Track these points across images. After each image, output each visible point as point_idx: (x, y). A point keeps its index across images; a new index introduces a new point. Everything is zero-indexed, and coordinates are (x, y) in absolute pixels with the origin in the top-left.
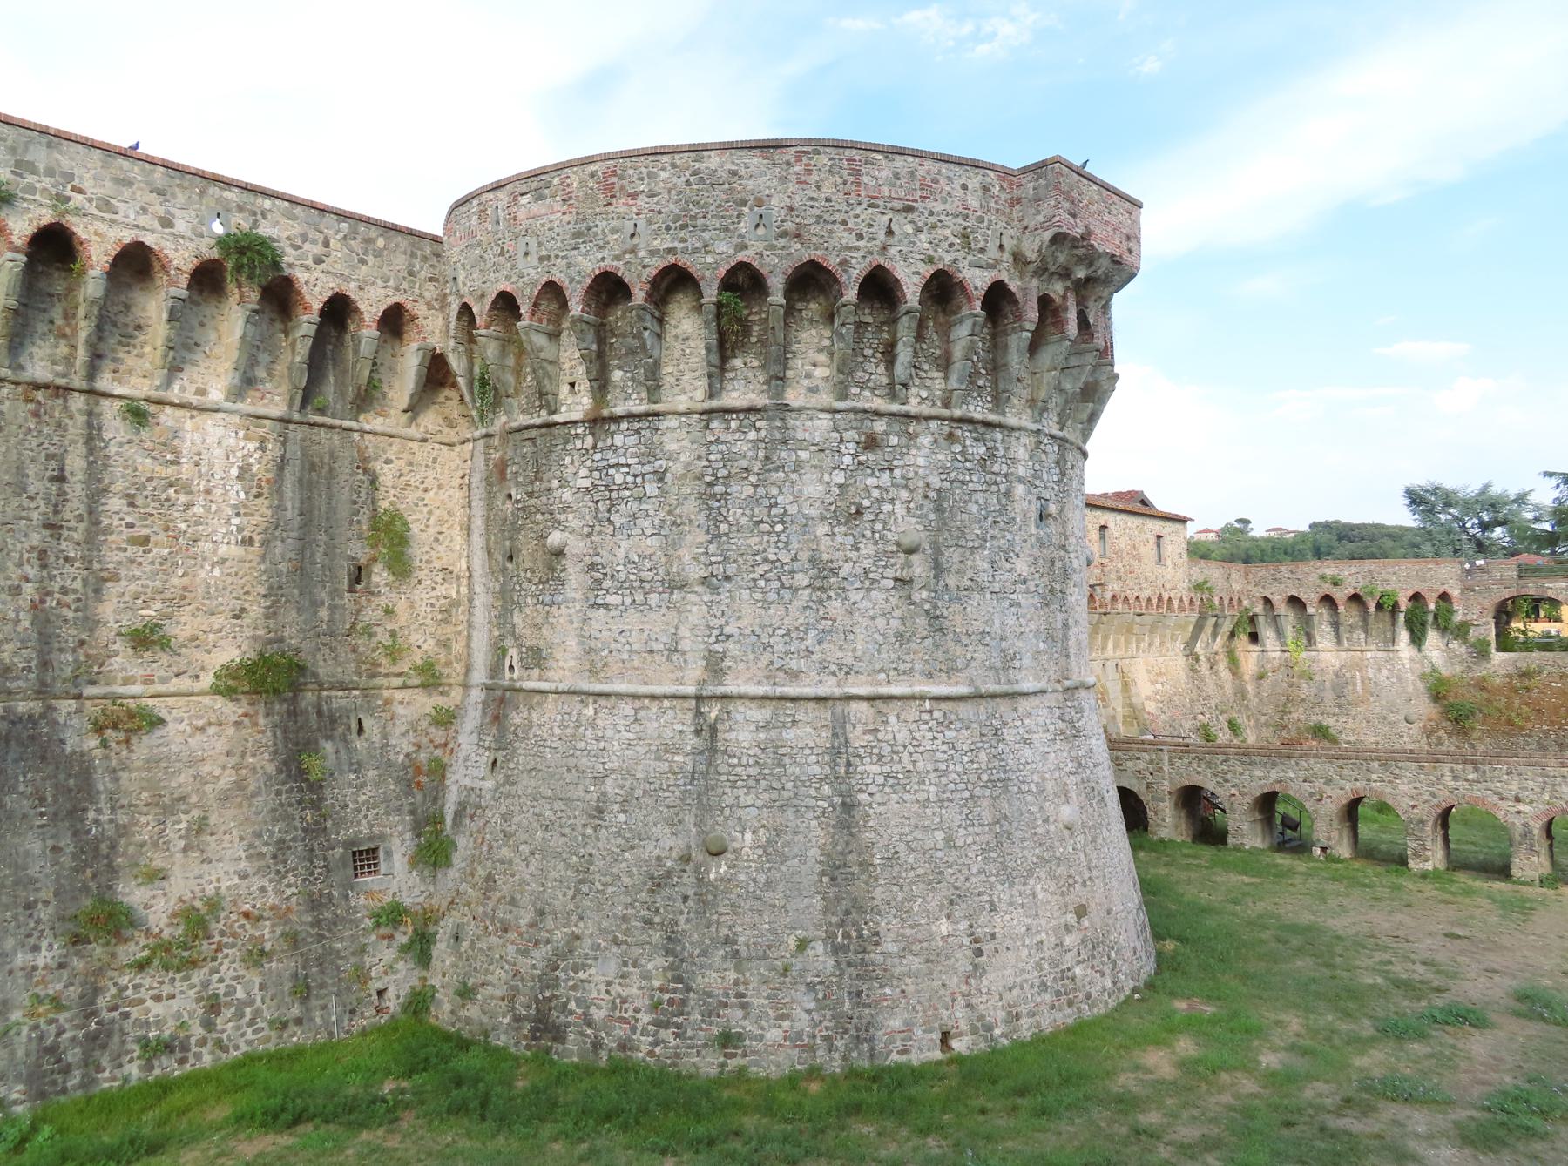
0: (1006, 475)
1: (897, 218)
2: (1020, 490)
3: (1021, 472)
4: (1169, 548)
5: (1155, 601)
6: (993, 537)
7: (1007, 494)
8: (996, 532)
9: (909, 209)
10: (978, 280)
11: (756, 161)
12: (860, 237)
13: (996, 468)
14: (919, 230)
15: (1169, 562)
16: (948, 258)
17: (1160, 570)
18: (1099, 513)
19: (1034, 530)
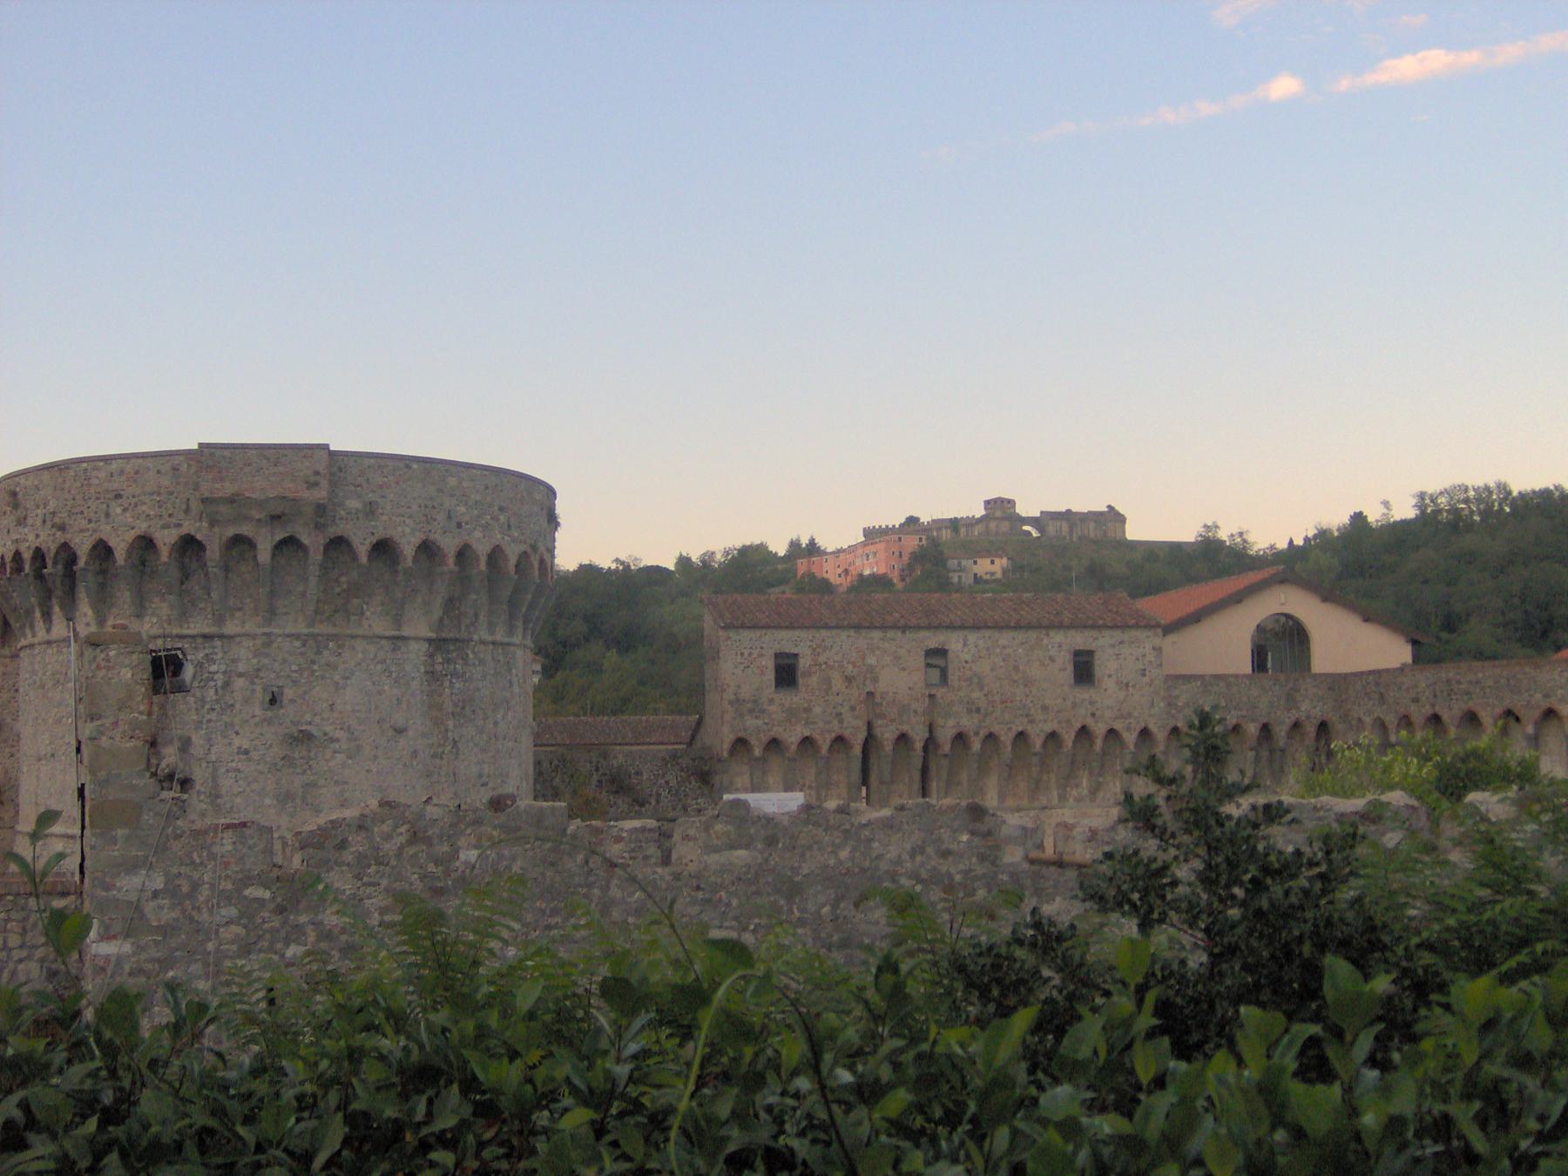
0: (225, 673)
1: (113, 504)
2: (239, 683)
3: (241, 667)
4: (1112, 665)
5: (1069, 738)
6: (210, 721)
7: (227, 684)
8: (213, 716)
9: (118, 496)
10: (166, 539)
11: (46, 476)
12: (90, 521)
13: (214, 668)
14: (125, 510)
15: (1110, 684)
16: (144, 526)
17: (1083, 694)
18: (923, 634)
19: (257, 712)
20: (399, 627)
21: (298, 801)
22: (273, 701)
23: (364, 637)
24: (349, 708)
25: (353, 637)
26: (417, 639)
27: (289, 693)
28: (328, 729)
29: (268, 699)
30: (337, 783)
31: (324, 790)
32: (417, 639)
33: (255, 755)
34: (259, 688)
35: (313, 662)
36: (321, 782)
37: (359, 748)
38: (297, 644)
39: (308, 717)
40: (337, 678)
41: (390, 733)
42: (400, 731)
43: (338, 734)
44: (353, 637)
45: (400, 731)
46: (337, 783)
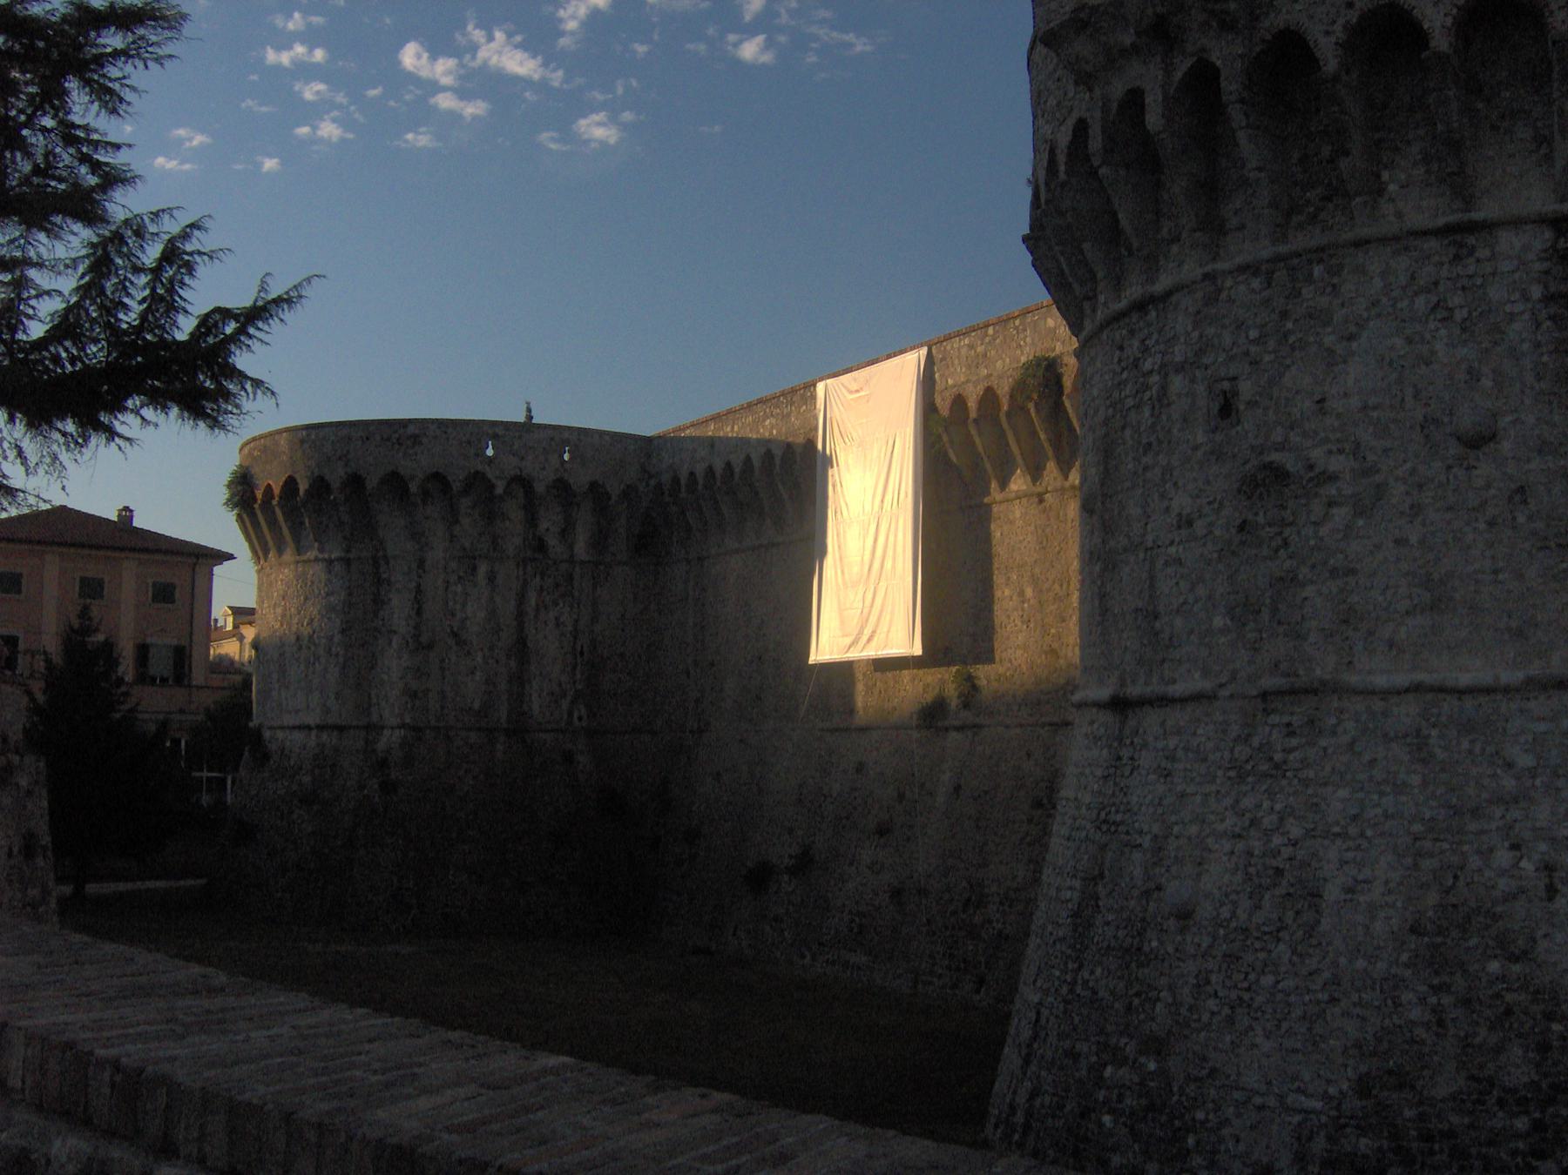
2: (1177, 383)
20: (1469, 203)
21: (1265, 615)
22: (1227, 409)
23: (1384, 240)
24: (1355, 402)
25: (1359, 244)
26: (1517, 223)
27: (1246, 389)
28: (1317, 454)
29: (1215, 407)
30: (1334, 573)
31: (1309, 591)
32: (1517, 223)
33: (1199, 527)
34: (1201, 389)
35: (1284, 315)
36: (1304, 572)
37: (1380, 490)
38: (1256, 283)
39: (1278, 435)
40: (1328, 340)
41: (1454, 449)
42: (1477, 442)
43: (1336, 464)
44: (1359, 244)
45: (1477, 442)
46: (1334, 573)
